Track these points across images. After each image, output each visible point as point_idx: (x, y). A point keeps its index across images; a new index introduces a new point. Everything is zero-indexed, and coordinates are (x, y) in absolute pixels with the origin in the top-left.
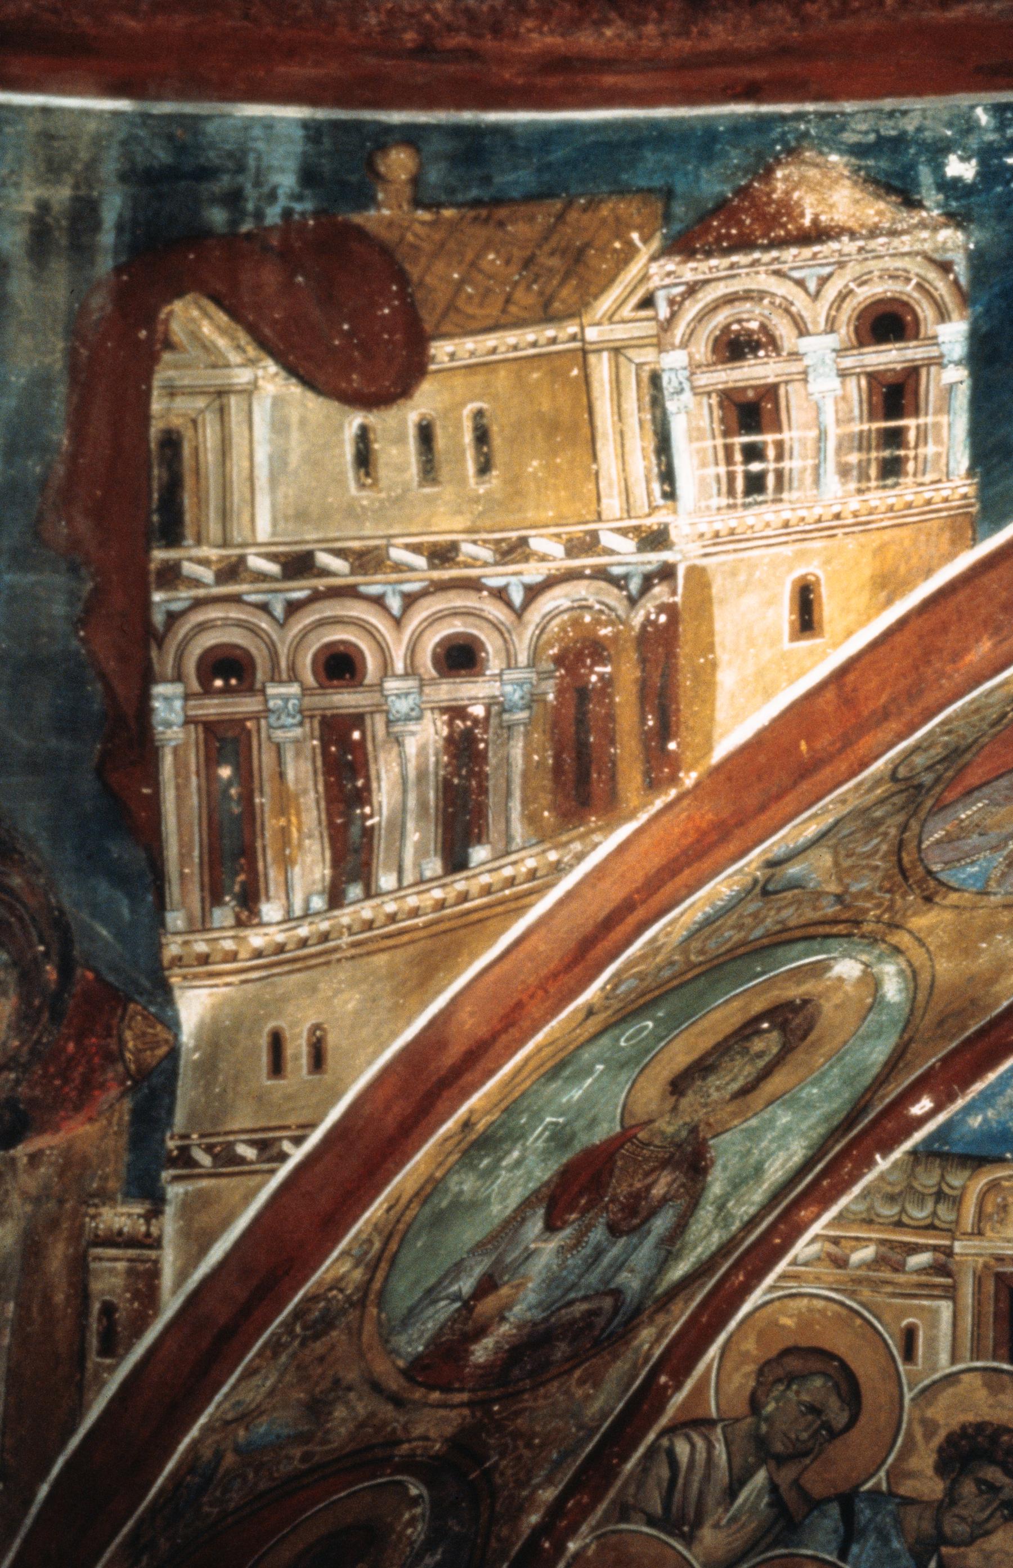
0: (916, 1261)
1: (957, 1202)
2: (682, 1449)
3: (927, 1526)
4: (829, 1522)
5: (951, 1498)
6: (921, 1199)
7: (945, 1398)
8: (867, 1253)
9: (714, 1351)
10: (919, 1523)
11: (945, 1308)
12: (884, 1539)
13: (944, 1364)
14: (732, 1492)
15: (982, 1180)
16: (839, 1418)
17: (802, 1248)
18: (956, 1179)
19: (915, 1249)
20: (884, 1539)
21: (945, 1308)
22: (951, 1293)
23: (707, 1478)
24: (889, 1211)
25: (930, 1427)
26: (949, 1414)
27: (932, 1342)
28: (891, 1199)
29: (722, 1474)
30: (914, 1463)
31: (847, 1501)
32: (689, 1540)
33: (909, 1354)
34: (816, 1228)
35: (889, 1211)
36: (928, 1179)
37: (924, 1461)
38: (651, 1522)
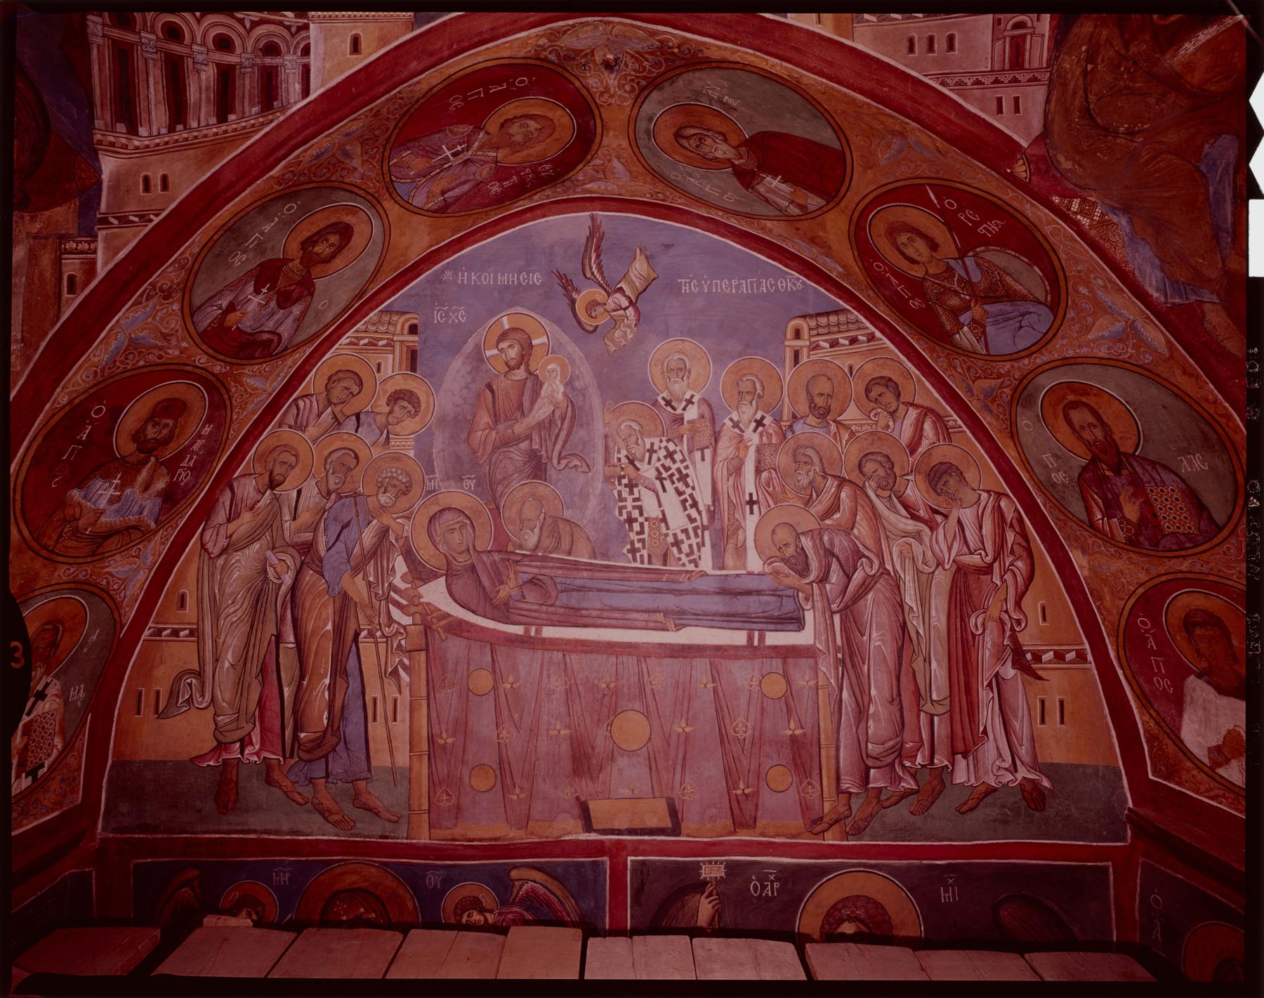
0: (381, 343)
1: (395, 325)
2: (301, 403)
3: (384, 420)
4: (350, 425)
5: (391, 412)
6: (383, 324)
7: (391, 383)
8: (366, 341)
9: (313, 372)
10: (381, 420)
11: (391, 356)
12: (370, 425)
13: (390, 374)
14: (319, 415)
15: (403, 319)
16: (355, 389)
17: (344, 340)
18: (395, 318)
19: (381, 339)
20: (370, 425)
21: (391, 356)
22: (393, 352)
23: (310, 411)
24: (374, 328)
25: (385, 392)
26: (391, 388)
27: (386, 366)
28: (374, 324)
29: (315, 411)
30: (380, 402)
31: (358, 416)
32: (304, 431)
33: (379, 371)
34: (349, 334)
35: (374, 328)
36: (386, 318)
37: (383, 401)
38: (290, 427)
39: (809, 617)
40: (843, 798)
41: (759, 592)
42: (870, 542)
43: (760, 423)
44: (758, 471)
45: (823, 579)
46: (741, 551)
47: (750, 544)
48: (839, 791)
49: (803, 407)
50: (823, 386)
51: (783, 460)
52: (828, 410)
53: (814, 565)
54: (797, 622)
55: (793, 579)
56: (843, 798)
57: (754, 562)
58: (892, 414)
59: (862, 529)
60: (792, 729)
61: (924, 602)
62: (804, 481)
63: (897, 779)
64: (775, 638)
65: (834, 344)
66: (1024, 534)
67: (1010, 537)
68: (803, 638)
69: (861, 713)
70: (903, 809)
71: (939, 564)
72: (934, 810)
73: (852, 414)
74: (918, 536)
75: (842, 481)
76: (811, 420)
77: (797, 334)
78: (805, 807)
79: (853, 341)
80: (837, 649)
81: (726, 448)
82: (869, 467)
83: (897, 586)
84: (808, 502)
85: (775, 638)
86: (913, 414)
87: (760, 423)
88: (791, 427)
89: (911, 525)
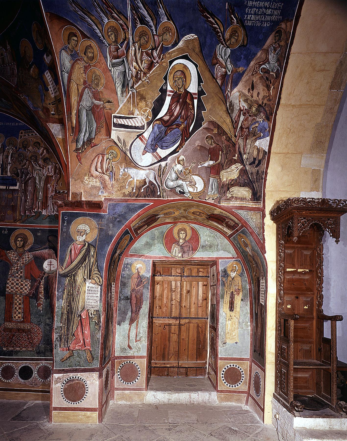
39: (18, 184)
40: (21, 216)
41: (9, 180)
42: (31, 171)
43: (12, 149)
44: (11, 158)
45: (21, 177)
46: (6, 172)
47: (8, 171)
48: (20, 215)
49: (21, 146)
50: (26, 143)
51: (16, 156)
52: (26, 147)
53: (20, 175)
54: (16, 185)
55: (15, 177)
56: (21, 216)
57: (9, 174)
58: (38, 149)
59: (30, 168)
60: (12, 204)
61: (40, 182)
62: (20, 160)
63: (31, 213)
64: (11, 188)
65: (29, 135)
66: (60, 170)
67: (57, 171)
68: (17, 188)
69: (26, 201)
70: (32, 219)
71: (44, 175)
72: (38, 219)
73: (30, 148)
74: (40, 170)
75: (27, 160)
76: (23, 149)
77: (22, 133)
78: (14, 217)
79: (32, 135)
80: (23, 190)
81: (5, 153)
82: (33, 158)
83: (35, 179)
84: (20, 164)
85: (11, 188)
86: (42, 148)
87: (12, 149)
88: (18, 150)
89: (39, 168)
